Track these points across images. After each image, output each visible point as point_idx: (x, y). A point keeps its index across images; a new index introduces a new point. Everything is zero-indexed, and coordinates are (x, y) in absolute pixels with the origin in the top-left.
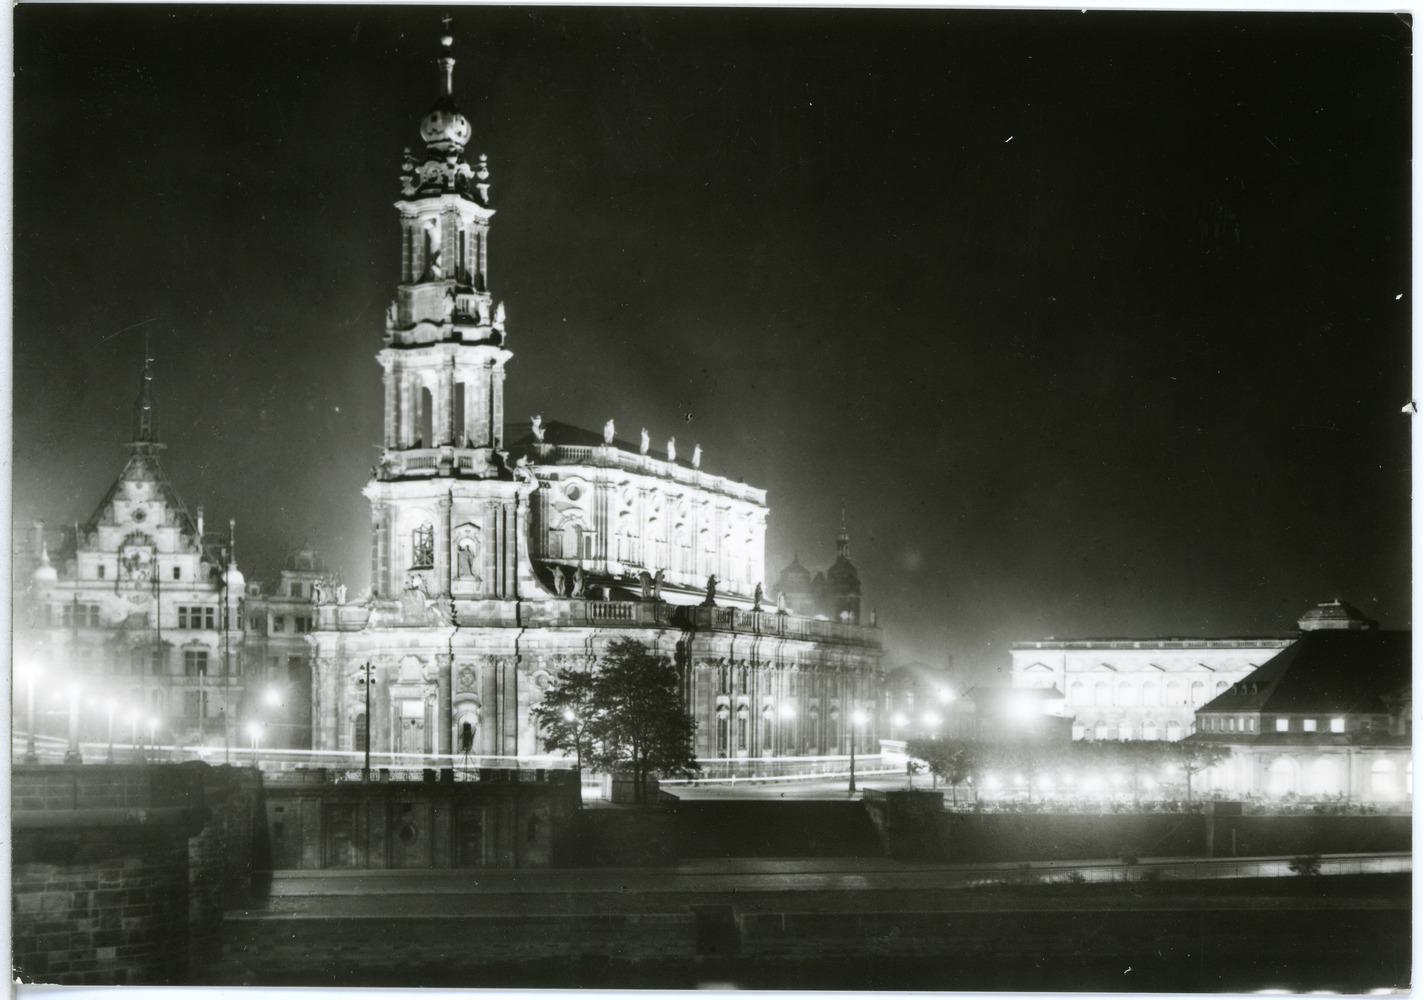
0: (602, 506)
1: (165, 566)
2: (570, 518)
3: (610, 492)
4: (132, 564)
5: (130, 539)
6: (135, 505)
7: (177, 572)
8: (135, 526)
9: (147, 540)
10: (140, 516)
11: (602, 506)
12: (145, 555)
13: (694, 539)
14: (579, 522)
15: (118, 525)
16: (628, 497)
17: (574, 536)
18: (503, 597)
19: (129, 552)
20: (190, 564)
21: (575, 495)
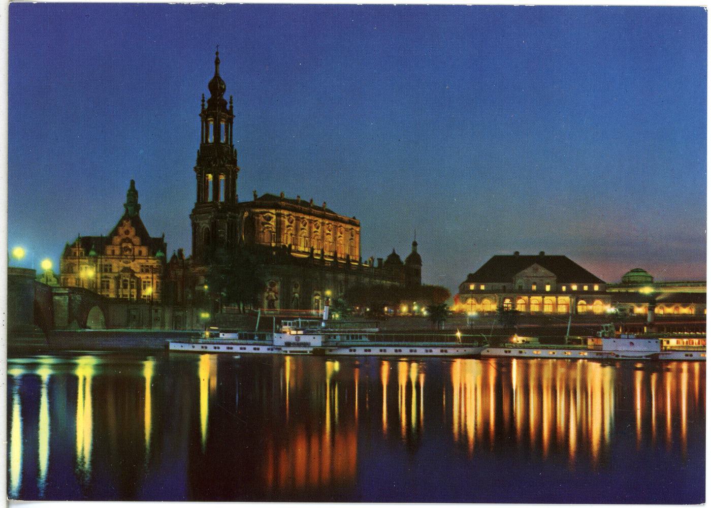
0: (279, 224)
1: (137, 250)
2: (267, 228)
3: (282, 219)
4: (127, 249)
5: (124, 241)
6: (126, 228)
7: (140, 252)
8: (125, 236)
9: (130, 241)
10: (127, 232)
11: (279, 224)
13: (323, 237)
14: (271, 229)
15: (120, 236)
16: (291, 220)
17: (269, 234)
19: (124, 245)
20: (144, 250)
21: (270, 218)
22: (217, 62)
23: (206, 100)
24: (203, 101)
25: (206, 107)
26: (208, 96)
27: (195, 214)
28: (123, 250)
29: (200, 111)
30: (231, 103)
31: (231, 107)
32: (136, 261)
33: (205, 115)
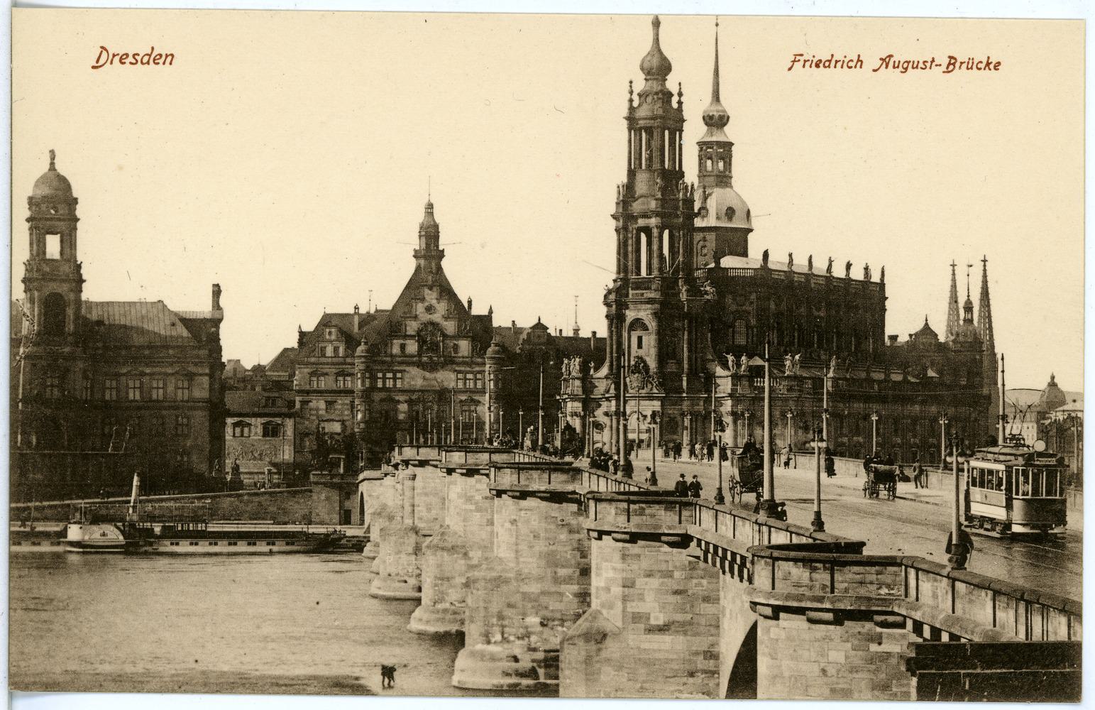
8: (425, 317)
24: (631, 93)
25: (635, 104)
26: (640, 84)
29: (625, 112)
30: (680, 94)
31: (680, 103)
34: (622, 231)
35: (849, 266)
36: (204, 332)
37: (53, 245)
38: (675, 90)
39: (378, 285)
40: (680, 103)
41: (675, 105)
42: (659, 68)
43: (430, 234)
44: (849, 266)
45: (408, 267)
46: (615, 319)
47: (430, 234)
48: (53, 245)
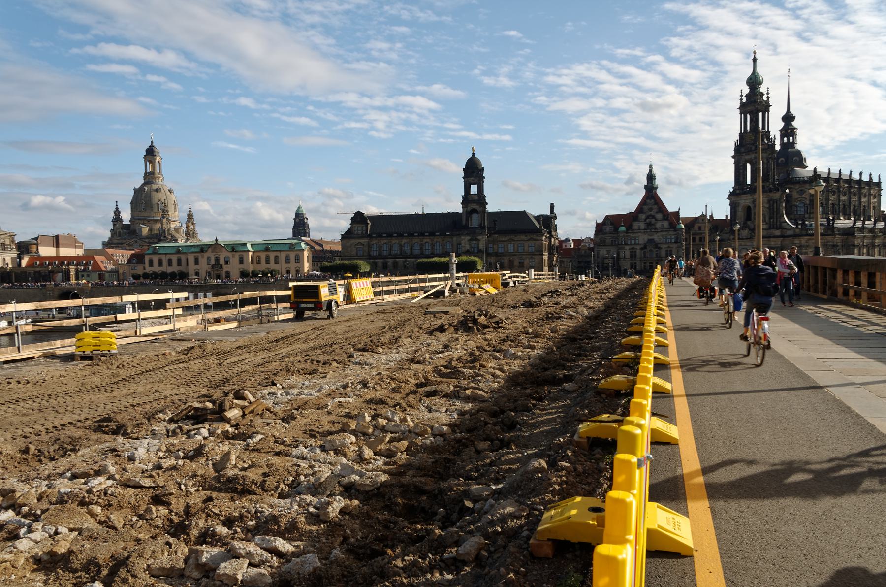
5: (648, 217)
9: (653, 217)
10: (651, 210)
12: (653, 221)
18: (777, 229)
19: (648, 220)
20: (666, 224)
22: (755, 60)
23: (744, 94)
24: (742, 96)
25: (744, 101)
26: (746, 90)
27: (732, 195)
28: (649, 225)
30: (768, 93)
31: (768, 97)
32: (659, 234)
33: (744, 108)
34: (737, 164)
35: (861, 174)
36: (548, 222)
37: (474, 189)
38: (765, 93)
39: (628, 202)
40: (768, 97)
41: (765, 99)
42: (754, 82)
43: (651, 177)
44: (861, 174)
45: (643, 193)
46: (733, 206)
47: (651, 177)
48: (474, 189)
